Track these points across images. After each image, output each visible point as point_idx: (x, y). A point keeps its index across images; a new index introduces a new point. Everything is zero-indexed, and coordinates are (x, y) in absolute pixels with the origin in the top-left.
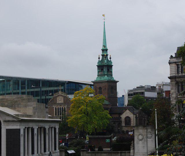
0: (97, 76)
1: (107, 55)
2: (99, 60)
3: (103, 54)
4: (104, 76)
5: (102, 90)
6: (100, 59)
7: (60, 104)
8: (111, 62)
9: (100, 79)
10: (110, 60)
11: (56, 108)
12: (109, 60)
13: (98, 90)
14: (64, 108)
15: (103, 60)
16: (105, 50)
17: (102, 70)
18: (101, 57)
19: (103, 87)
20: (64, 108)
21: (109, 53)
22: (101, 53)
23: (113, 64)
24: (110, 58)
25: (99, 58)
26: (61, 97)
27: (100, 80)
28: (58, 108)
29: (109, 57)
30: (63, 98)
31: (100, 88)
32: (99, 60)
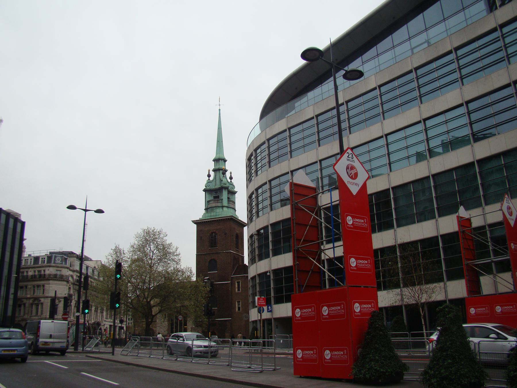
0: (204, 211)
1: (226, 171)
2: (209, 179)
3: (217, 167)
6: (211, 178)
8: (233, 185)
10: (231, 182)
12: (229, 180)
16: (219, 160)
17: (217, 198)
18: (212, 174)
21: (228, 166)
22: (212, 166)
23: (236, 190)
24: (231, 178)
25: (209, 176)
29: (228, 175)
32: (209, 179)
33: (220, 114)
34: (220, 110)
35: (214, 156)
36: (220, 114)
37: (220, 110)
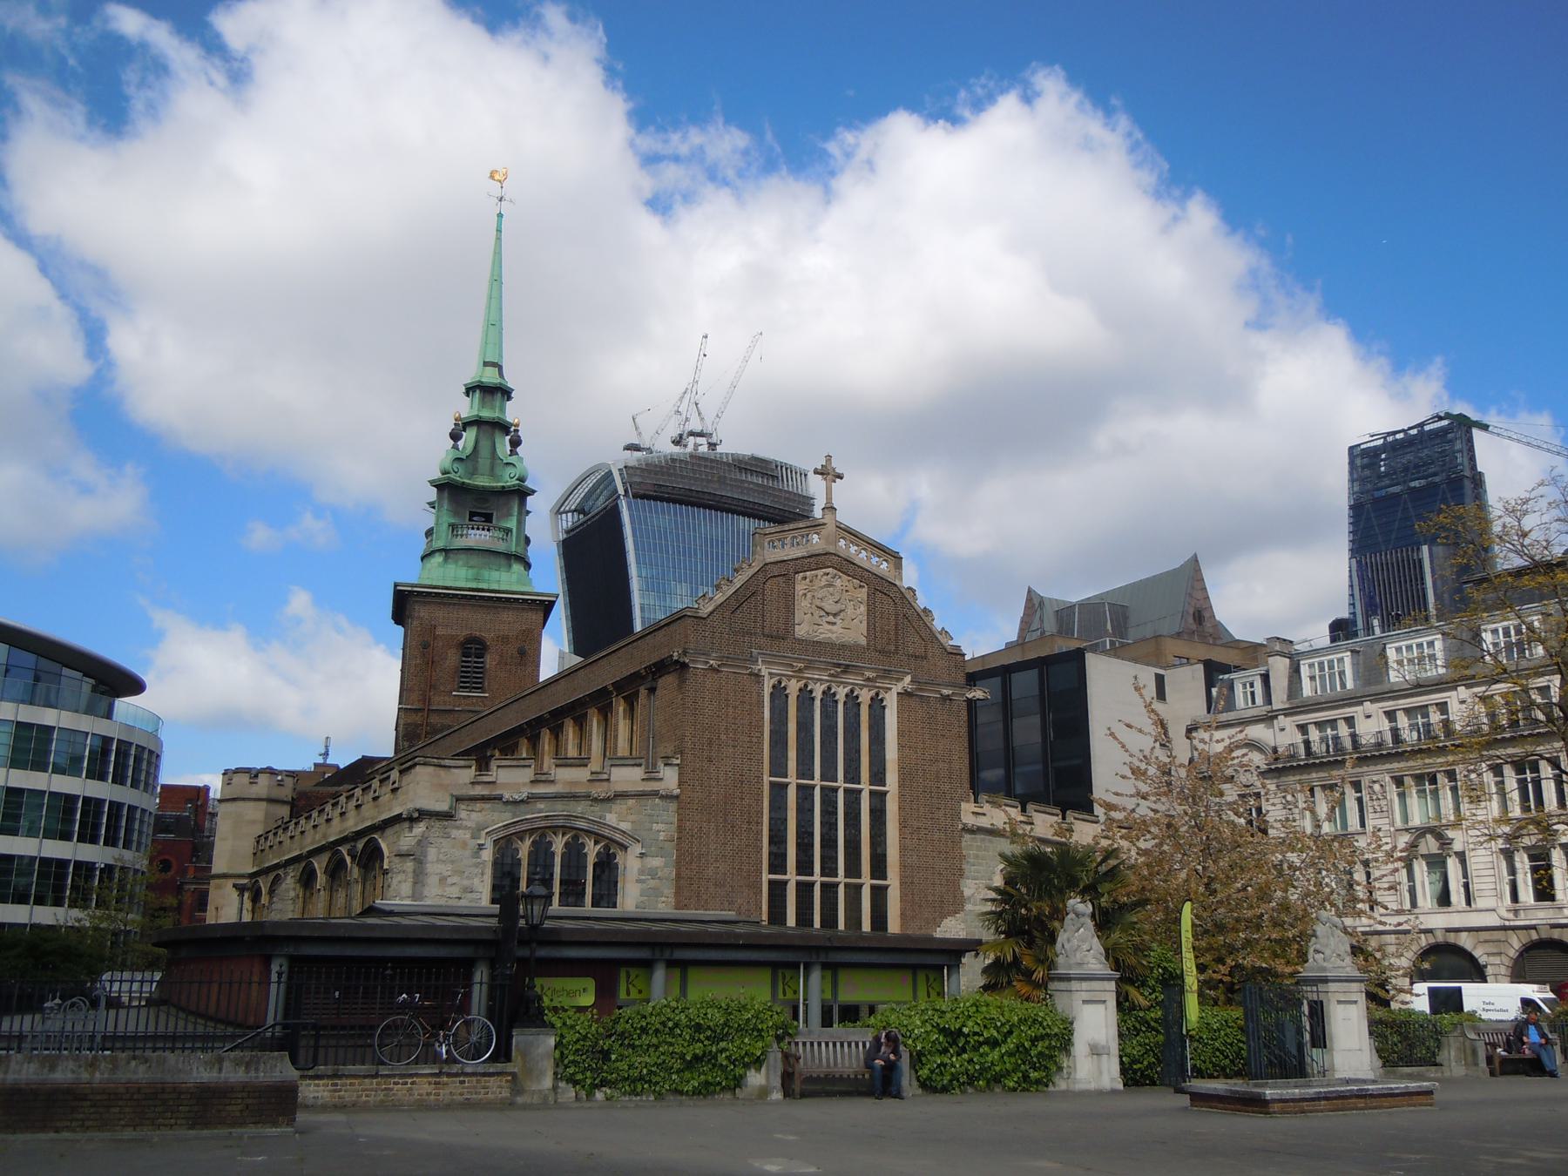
4: (503, 561)
5: (490, 660)
7: (841, 659)
9: (477, 579)
11: (779, 692)
13: (453, 658)
14: (865, 696)
15: (485, 451)
19: (505, 639)
20: (865, 696)
25: (455, 436)
26: (841, 582)
27: (474, 585)
28: (805, 696)
30: (863, 594)
31: (473, 648)
33: (499, 231)
34: (500, 215)
35: (473, 372)
36: (499, 231)
37: (500, 215)
